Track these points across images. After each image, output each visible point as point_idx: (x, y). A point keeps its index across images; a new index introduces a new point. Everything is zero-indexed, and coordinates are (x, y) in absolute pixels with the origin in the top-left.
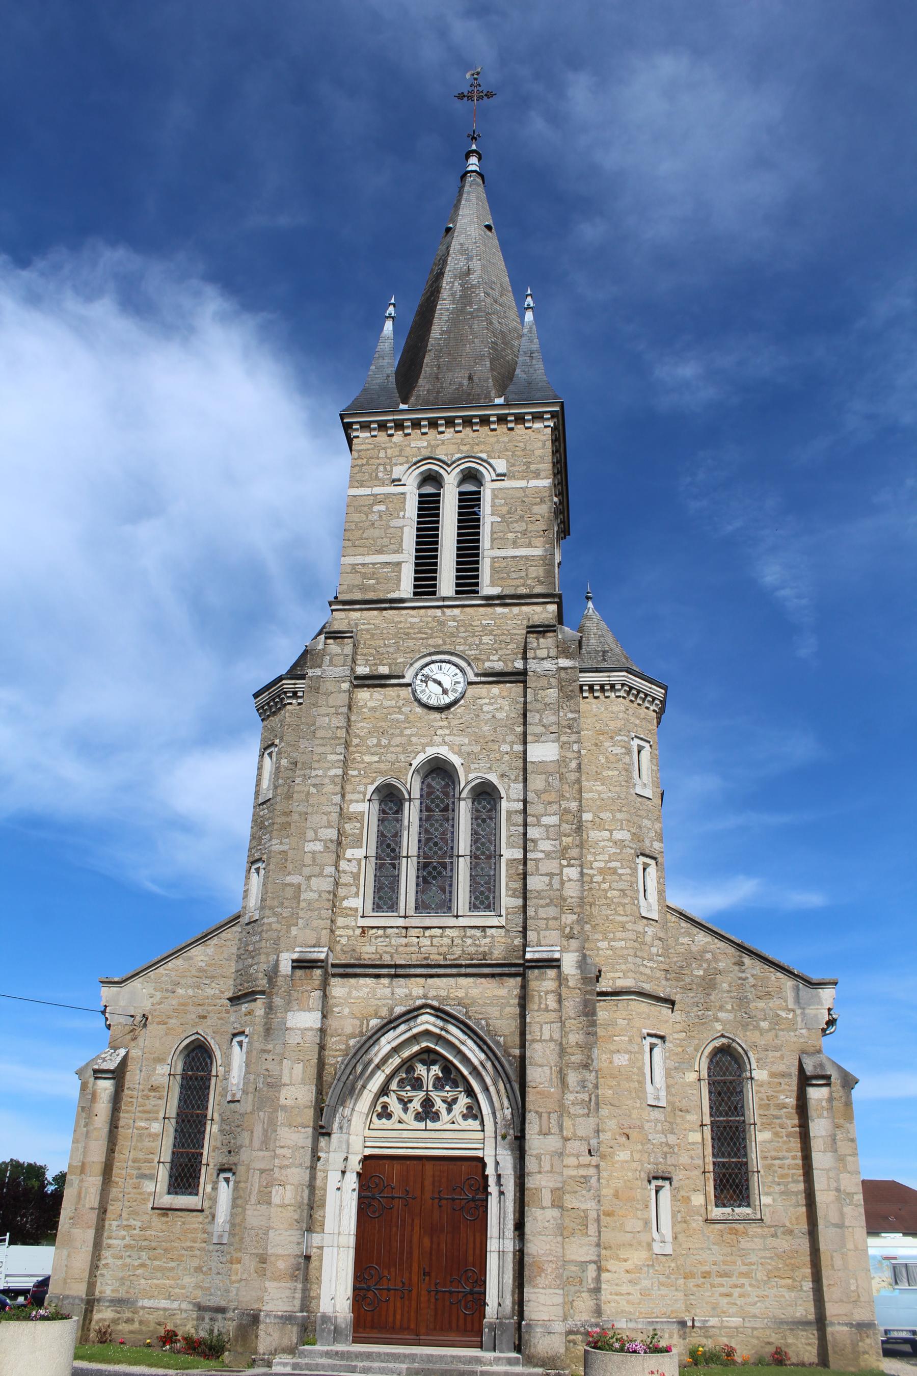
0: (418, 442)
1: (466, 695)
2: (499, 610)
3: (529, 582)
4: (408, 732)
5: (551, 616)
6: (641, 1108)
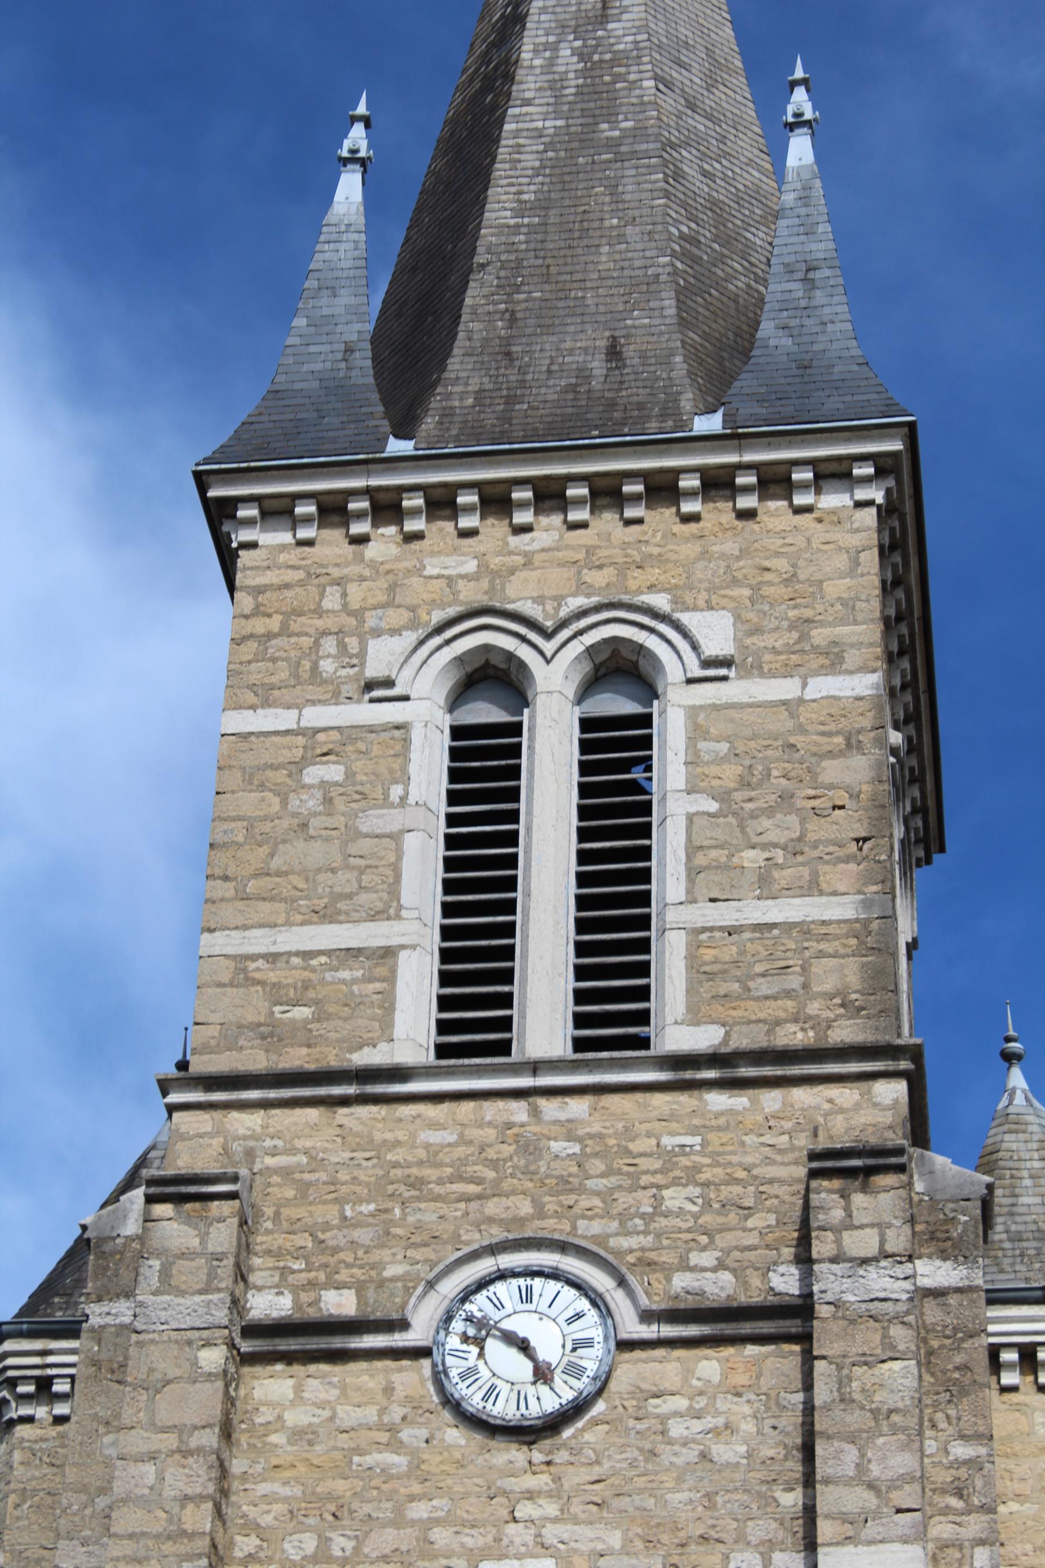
0: (449, 561)
1: (613, 1386)
2: (718, 1100)
3: (813, 1008)
4: (419, 1511)
5: (887, 1118)
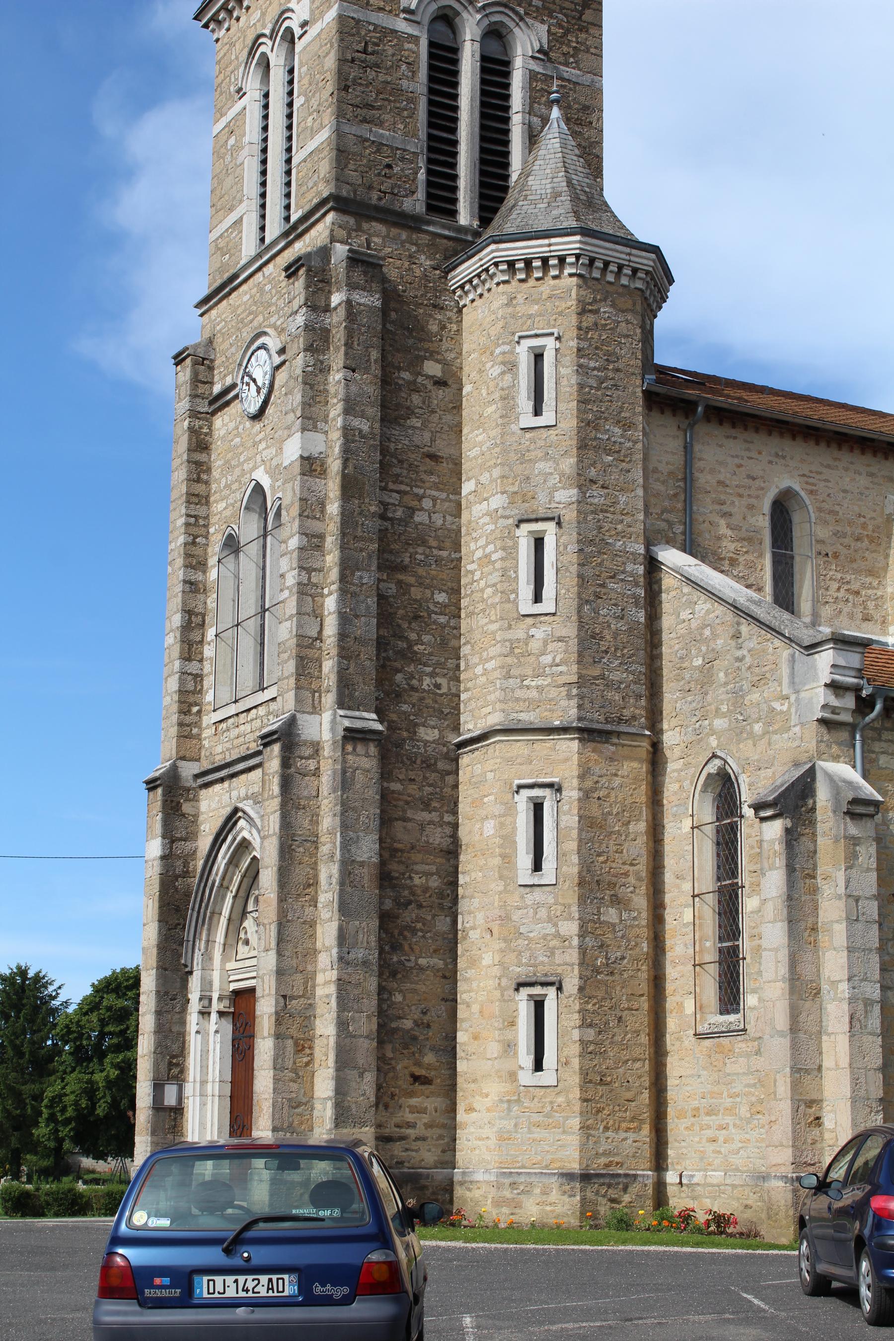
1: (276, 387)
6: (506, 891)
